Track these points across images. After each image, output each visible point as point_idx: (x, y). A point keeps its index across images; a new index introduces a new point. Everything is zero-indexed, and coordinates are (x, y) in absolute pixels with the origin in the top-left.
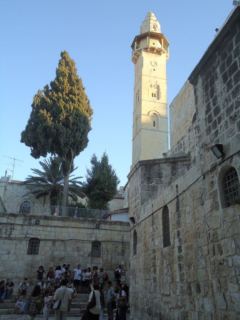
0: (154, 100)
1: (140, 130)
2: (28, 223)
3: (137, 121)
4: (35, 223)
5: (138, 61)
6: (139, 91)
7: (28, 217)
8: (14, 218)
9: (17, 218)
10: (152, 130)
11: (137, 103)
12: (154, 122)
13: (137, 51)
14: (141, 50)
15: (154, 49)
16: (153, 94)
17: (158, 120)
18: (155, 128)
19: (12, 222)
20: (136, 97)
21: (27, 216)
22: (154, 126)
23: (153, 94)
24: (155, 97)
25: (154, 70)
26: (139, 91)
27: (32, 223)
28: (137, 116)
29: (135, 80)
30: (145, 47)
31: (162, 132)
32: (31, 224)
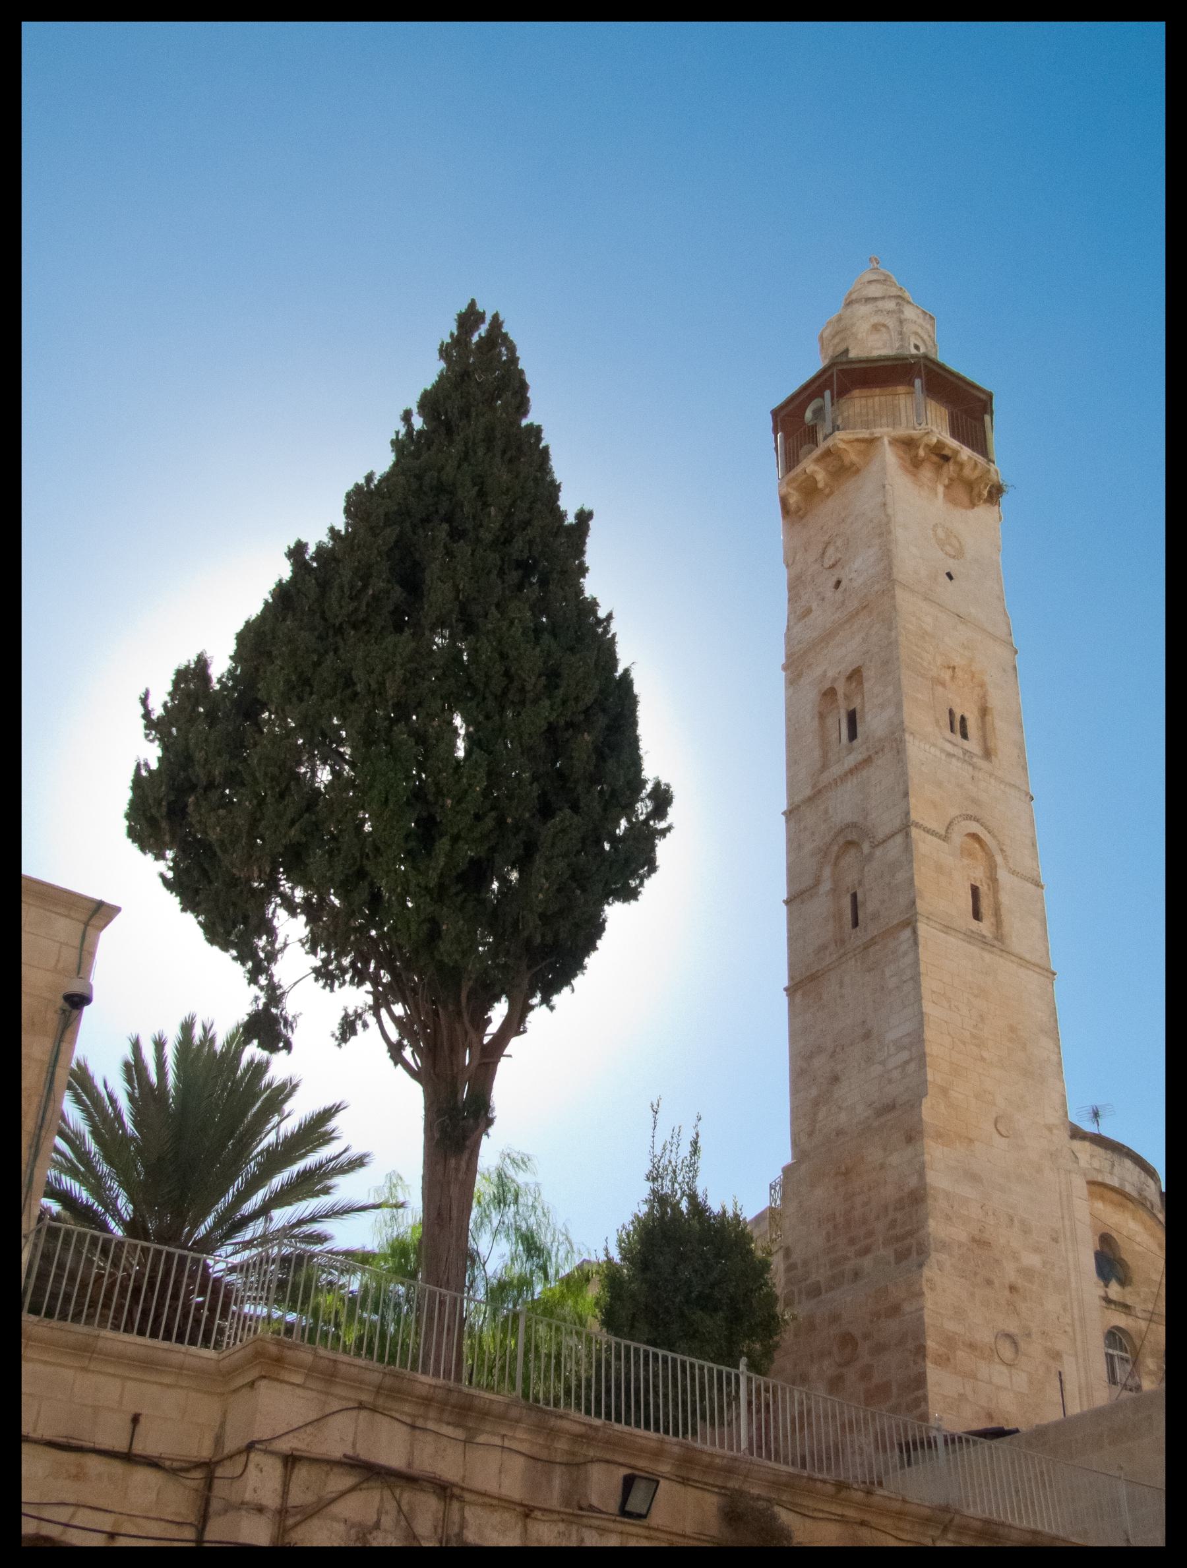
0: (966, 752)
1: (910, 923)
2: (567, 1500)
3: (835, 864)
4: (613, 1506)
5: (826, 512)
6: (855, 676)
7: (562, 1445)
8: (460, 1434)
9: (481, 1439)
10: (972, 937)
11: (825, 755)
12: (975, 891)
13: (849, 442)
14: (871, 441)
15: (946, 459)
16: (951, 713)
17: (993, 880)
18: (985, 927)
19: (448, 1468)
20: (822, 716)
21: (553, 1434)
22: (977, 915)
23: (951, 713)
24: (965, 736)
25: (950, 576)
26: (855, 676)
27: (595, 1502)
28: (854, 836)
29: (799, 612)
30: (902, 432)
31: (1023, 962)
32: (591, 1508)
